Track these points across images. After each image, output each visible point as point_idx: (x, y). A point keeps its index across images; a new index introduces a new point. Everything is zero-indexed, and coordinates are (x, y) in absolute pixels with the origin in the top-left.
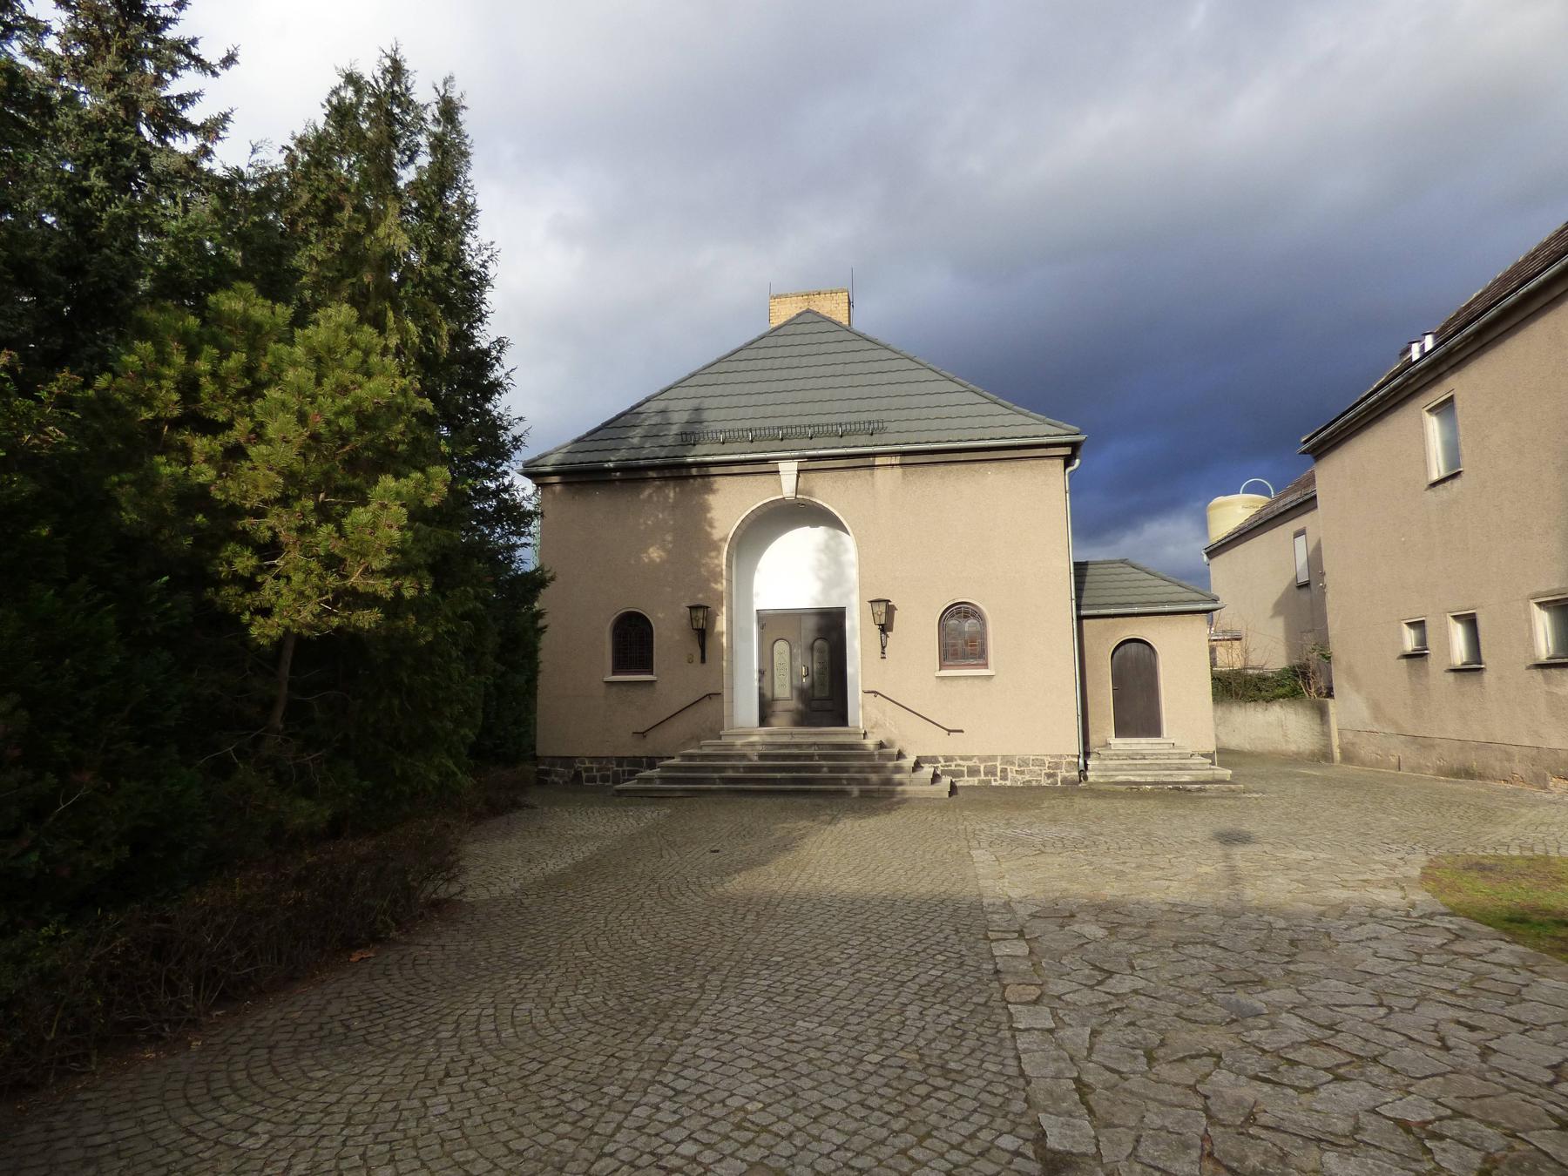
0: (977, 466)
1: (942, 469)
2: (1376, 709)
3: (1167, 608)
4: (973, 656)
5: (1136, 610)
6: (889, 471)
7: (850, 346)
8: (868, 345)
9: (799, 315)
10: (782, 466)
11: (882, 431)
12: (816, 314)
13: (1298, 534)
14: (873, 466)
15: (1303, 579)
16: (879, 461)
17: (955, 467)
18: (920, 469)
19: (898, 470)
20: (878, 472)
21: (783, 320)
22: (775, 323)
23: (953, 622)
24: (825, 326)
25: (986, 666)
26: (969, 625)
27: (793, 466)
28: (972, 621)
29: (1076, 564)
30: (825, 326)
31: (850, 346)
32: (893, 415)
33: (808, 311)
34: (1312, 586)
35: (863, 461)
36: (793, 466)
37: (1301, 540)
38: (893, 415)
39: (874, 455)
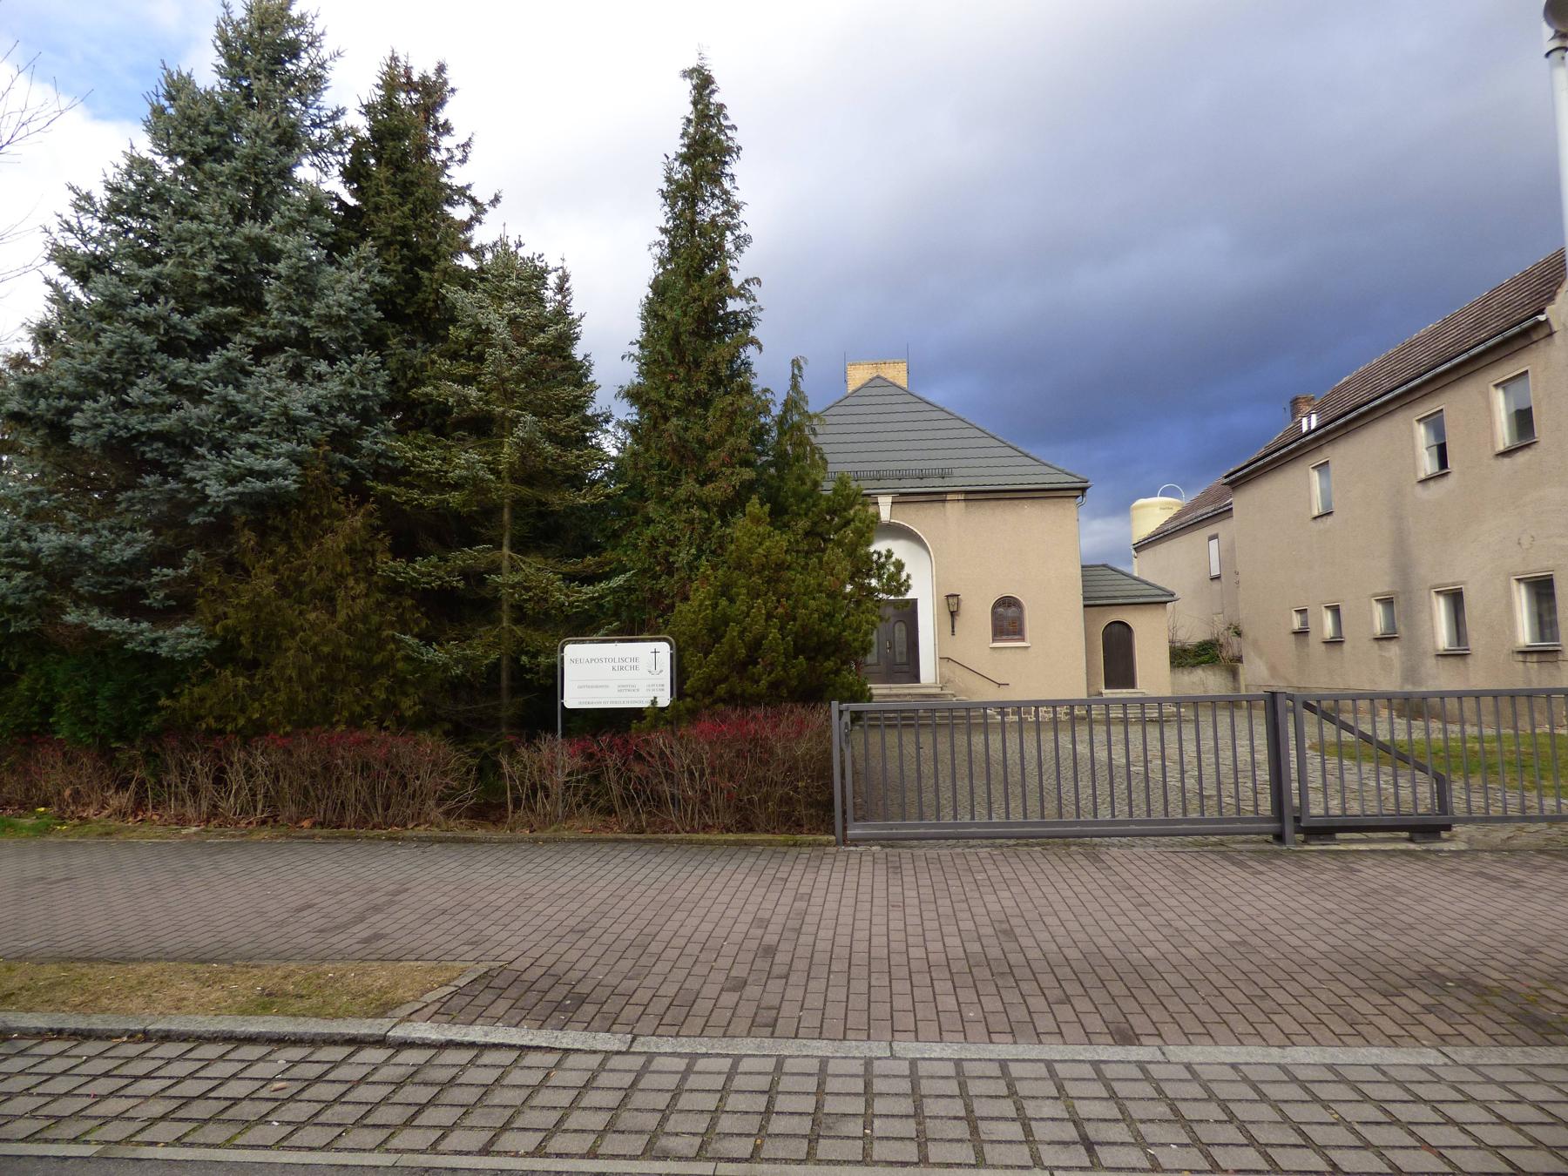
0: (1016, 502)
1: (993, 503)
2: (1273, 669)
3: (1141, 600)
4: (1015, 633)
5: (1120, 601)
6: (956, 505)
7: (914, 407)
8: (928, 407)
9: (872, 380)
10: (881, 499)
11: (951, 476)
12: (885, 379)
13: (1212, 538)
14: (944, 501)
15: (1215, 572)
16: (949, 497)
17: (1002, 502)
18: (977, 503)
19: (962, 504)
20: (948, 505)
21: (858, 384)
22: (851, 389)
23: (1001, 610)
24: (892, 390)
25: (1023, 640)
26: (1011, 612)
27: (889, 499)
28: (1013, 609)
29: (1083, 567)
30: (892, 390)
31: (914, 407)
32: (957, 463)
33: (878, 377)
34: (1223, 578)
35: (937, 497)
36: (889, 499)
37: (1214, 543)
38: (957, 463)
39: (946, 493)
